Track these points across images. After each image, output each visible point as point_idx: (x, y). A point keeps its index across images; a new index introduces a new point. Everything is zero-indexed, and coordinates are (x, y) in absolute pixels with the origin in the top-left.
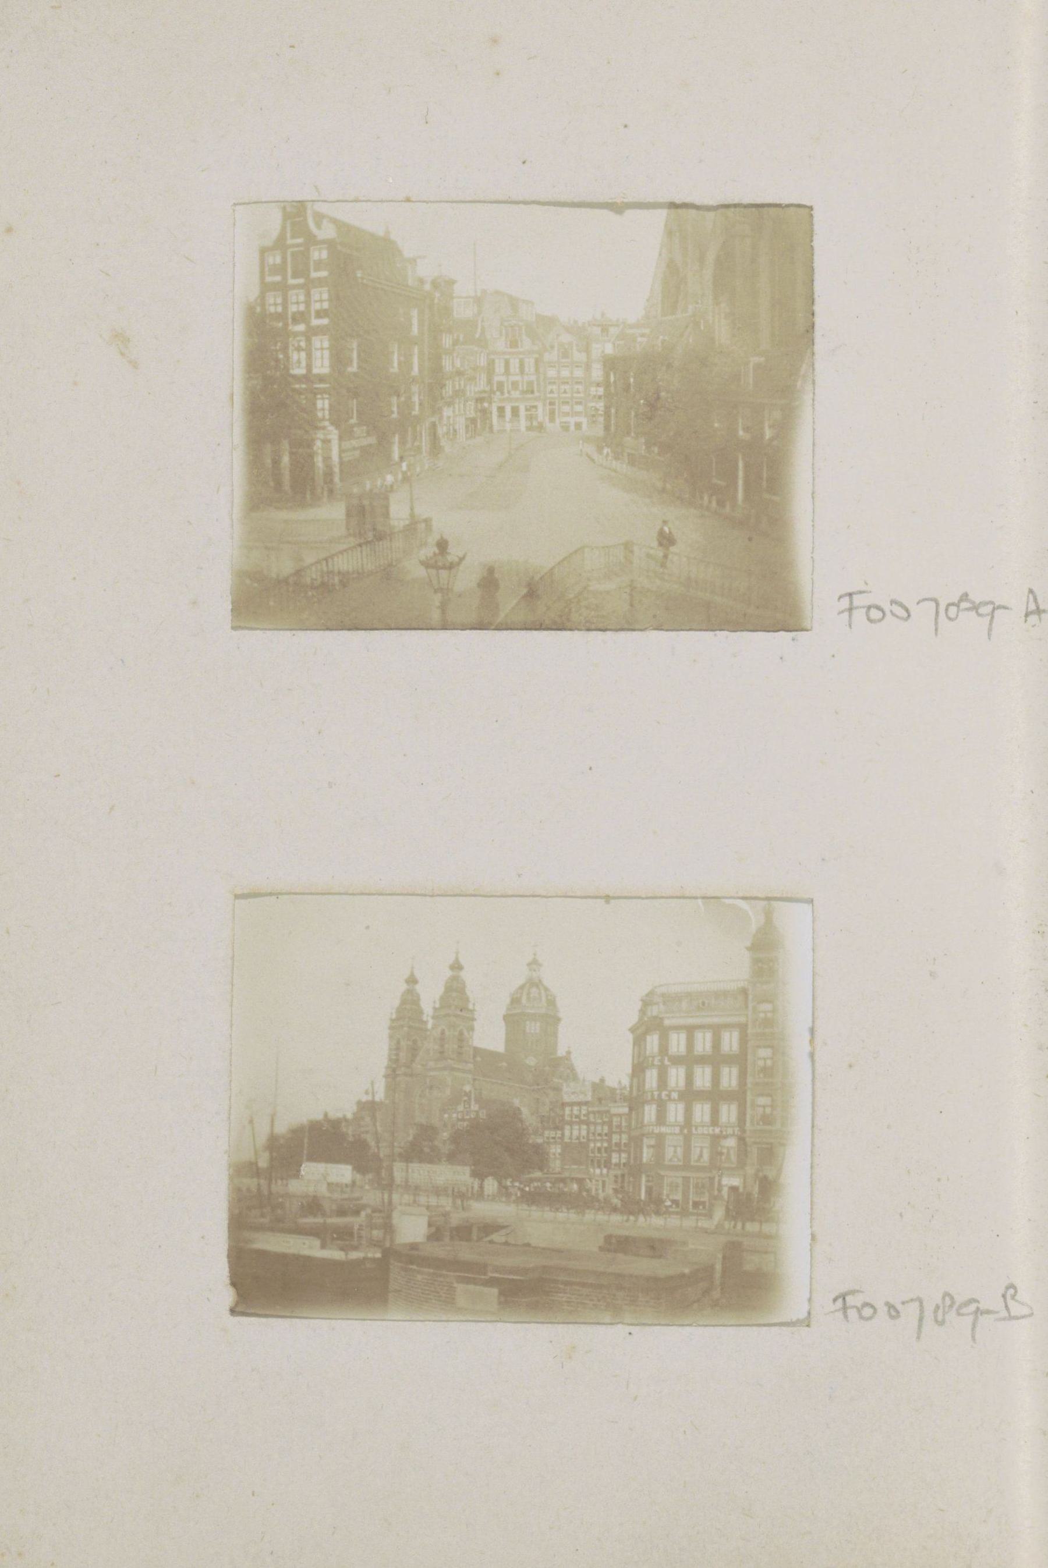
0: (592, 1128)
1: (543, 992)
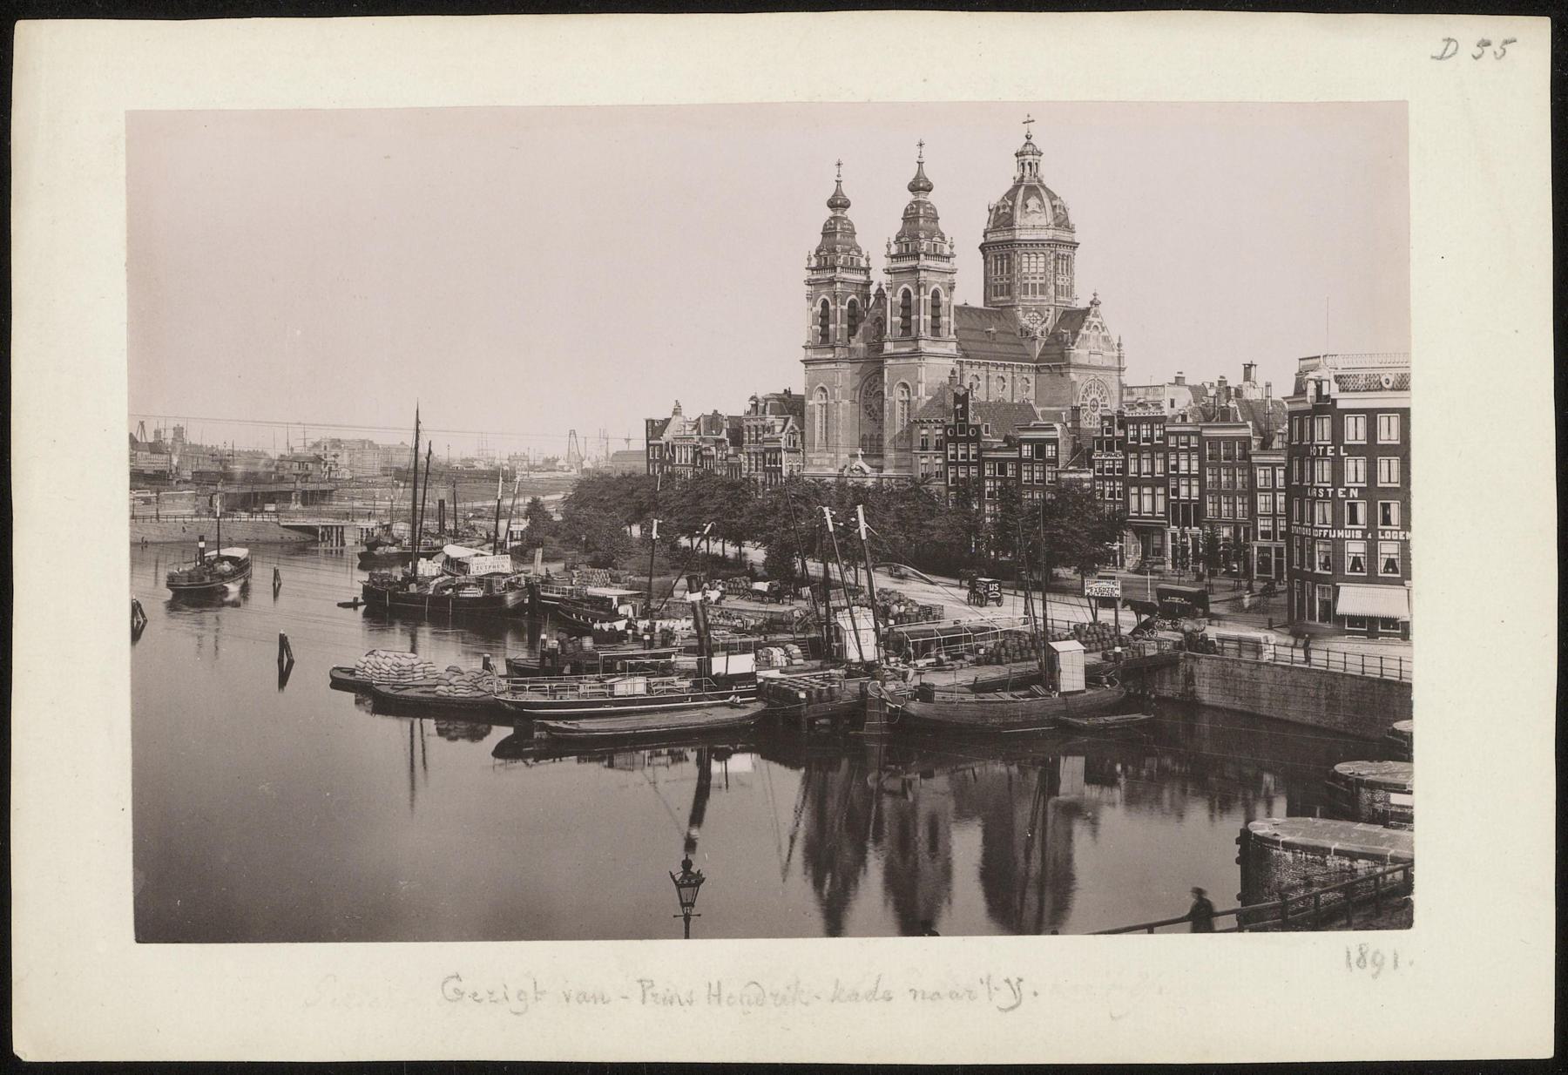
1: (1046, 200)
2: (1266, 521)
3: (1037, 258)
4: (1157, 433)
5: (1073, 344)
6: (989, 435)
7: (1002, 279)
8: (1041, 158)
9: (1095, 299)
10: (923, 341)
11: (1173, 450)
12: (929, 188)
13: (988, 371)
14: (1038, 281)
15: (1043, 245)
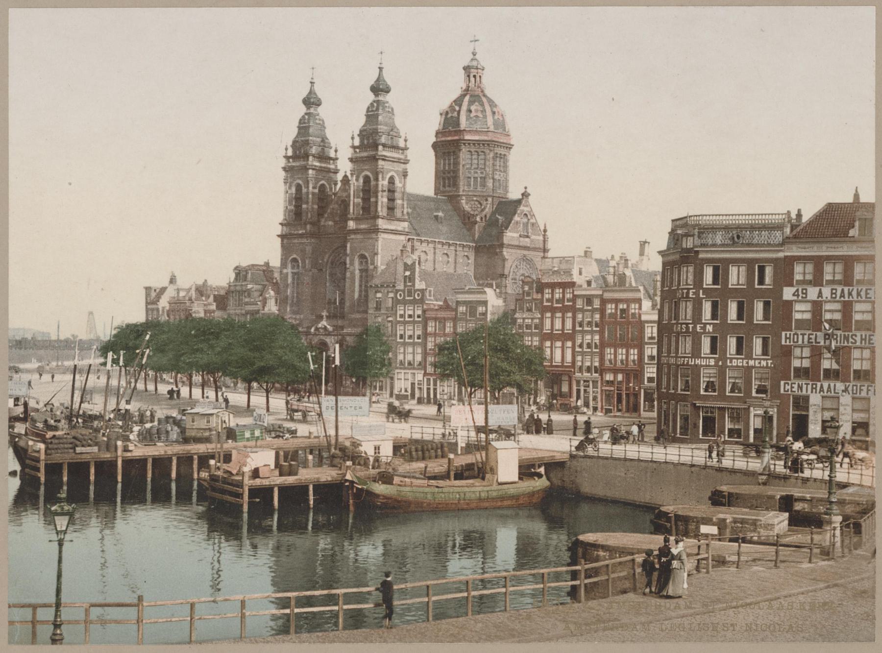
0: (579, 316)
2: (651, 369)
3: (478, 155)
4: (568, 296)
5: (507, 228)
6: (432, 298)
7: (449, 173)
8: (484, 72)
9: (526, 192)
10: (380, 220)
11: (580, 309)
12: (387, 90)
13: (435, 248)
14: (479, 175)
15: (483, 144)
